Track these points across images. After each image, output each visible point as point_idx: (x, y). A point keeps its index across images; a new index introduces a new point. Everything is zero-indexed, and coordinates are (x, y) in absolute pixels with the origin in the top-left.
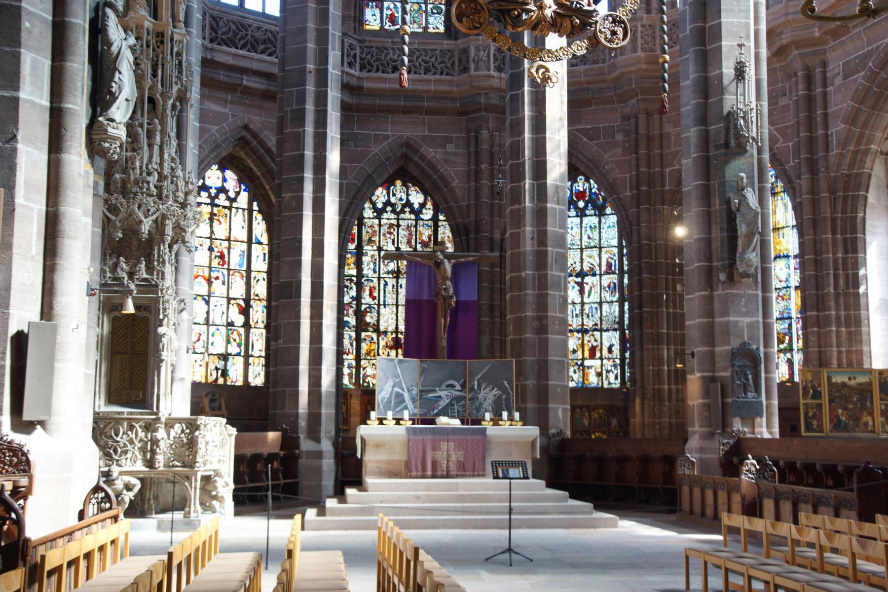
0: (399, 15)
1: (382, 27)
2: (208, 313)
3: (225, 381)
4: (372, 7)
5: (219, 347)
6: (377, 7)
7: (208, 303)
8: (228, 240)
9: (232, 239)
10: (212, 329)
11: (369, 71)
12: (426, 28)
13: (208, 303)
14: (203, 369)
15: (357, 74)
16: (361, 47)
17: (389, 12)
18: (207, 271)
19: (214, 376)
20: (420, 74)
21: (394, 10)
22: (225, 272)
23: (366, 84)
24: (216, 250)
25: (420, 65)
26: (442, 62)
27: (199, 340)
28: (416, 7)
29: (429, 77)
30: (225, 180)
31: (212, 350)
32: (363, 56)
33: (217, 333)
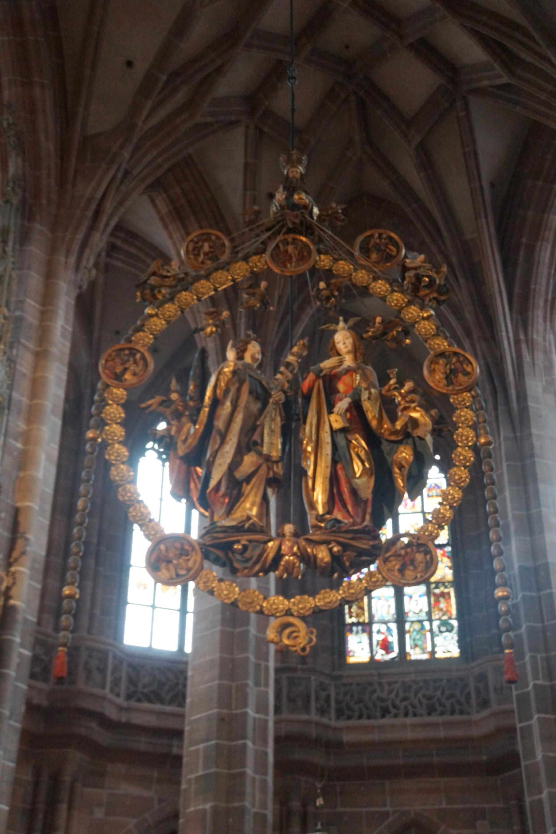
0: (394, 639)
1: (372, 657)
4: (357, 632)
6: (363, 631)
11: (349, 718)
12: (433, 653)
15: (333, 723)
16: (336, 686)
17: (381, 637)
20: (421, 715)
21: (387, 633)
23: (346, 738)
25: (421, 703)
26: (452, 696)
28: (417, 626)
29: (435, 718)
32: (340, 697)
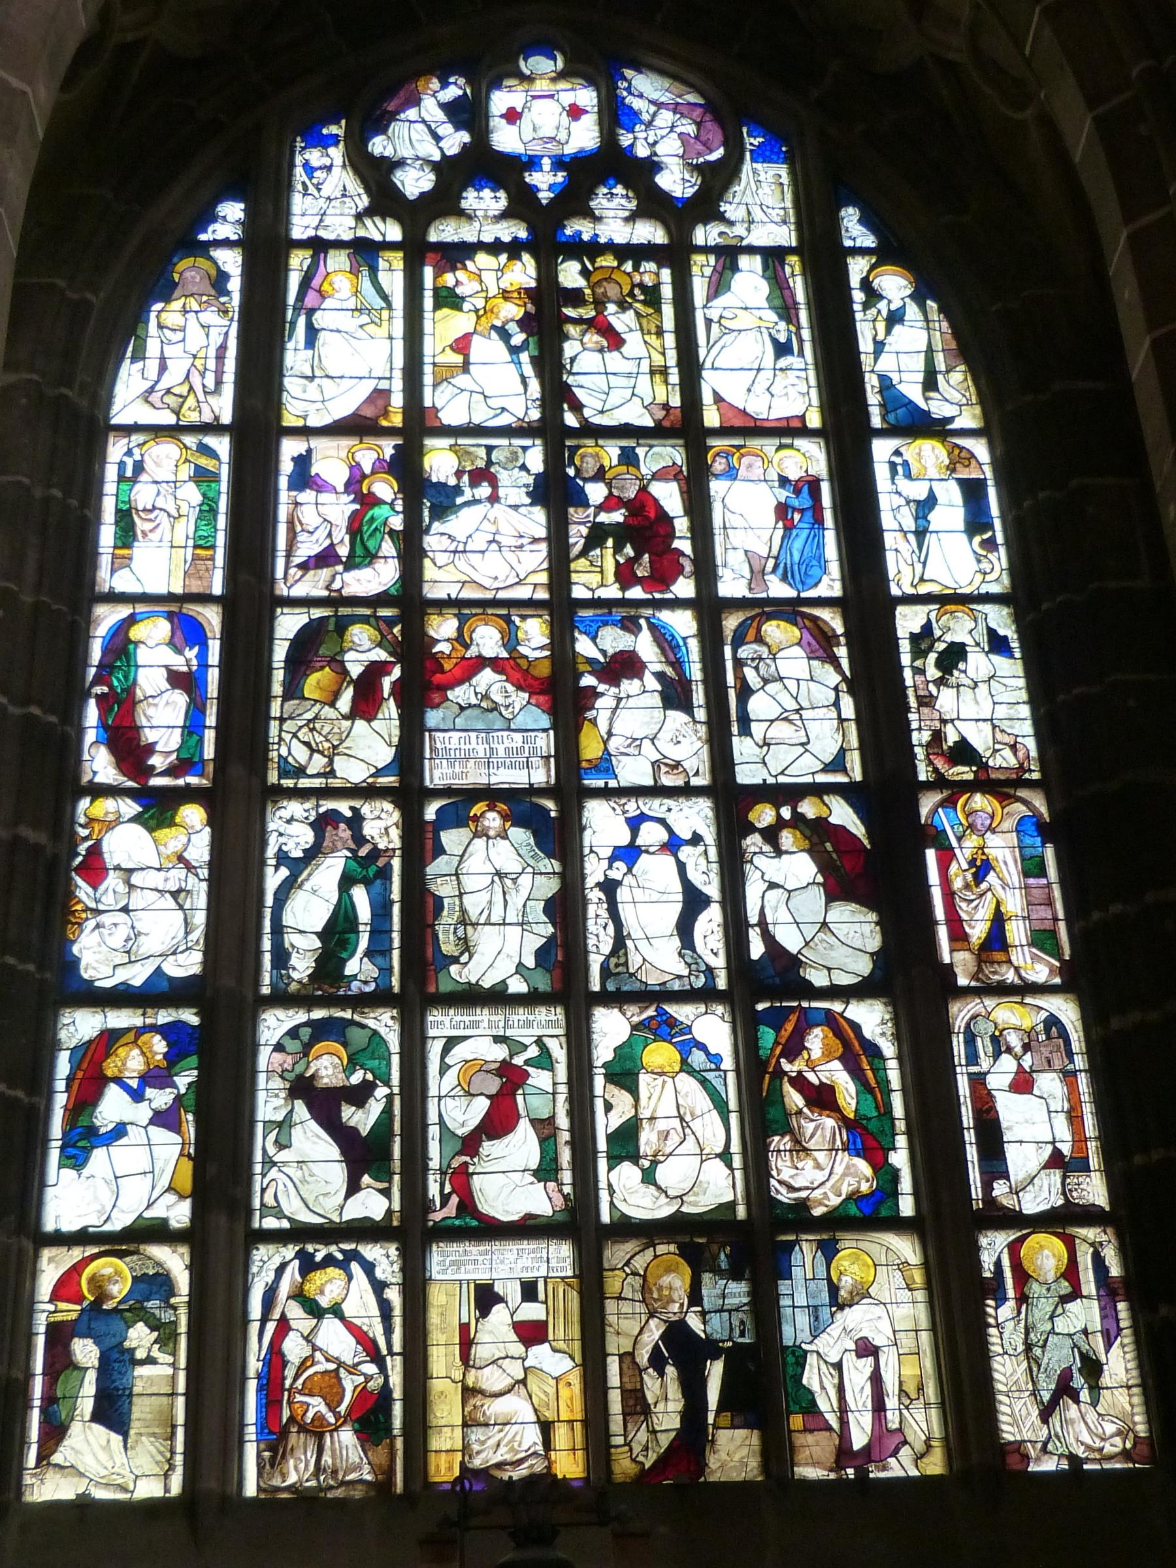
2: (566, 909)
3: (777, 1452)
5: (688, 1162)
7: (560, 837)
8: (684, 425)
9: (711, 418)
10: (611, 1028)
13: (560, 837)
14: (554, 1362)
18: (535, 634)
19: (668, 1415)
22: (683, 623)
24: (596, 492)
27: (498, 1122)
30: (614, 115)
31: (626, 1192)
33: (660, 1054)
